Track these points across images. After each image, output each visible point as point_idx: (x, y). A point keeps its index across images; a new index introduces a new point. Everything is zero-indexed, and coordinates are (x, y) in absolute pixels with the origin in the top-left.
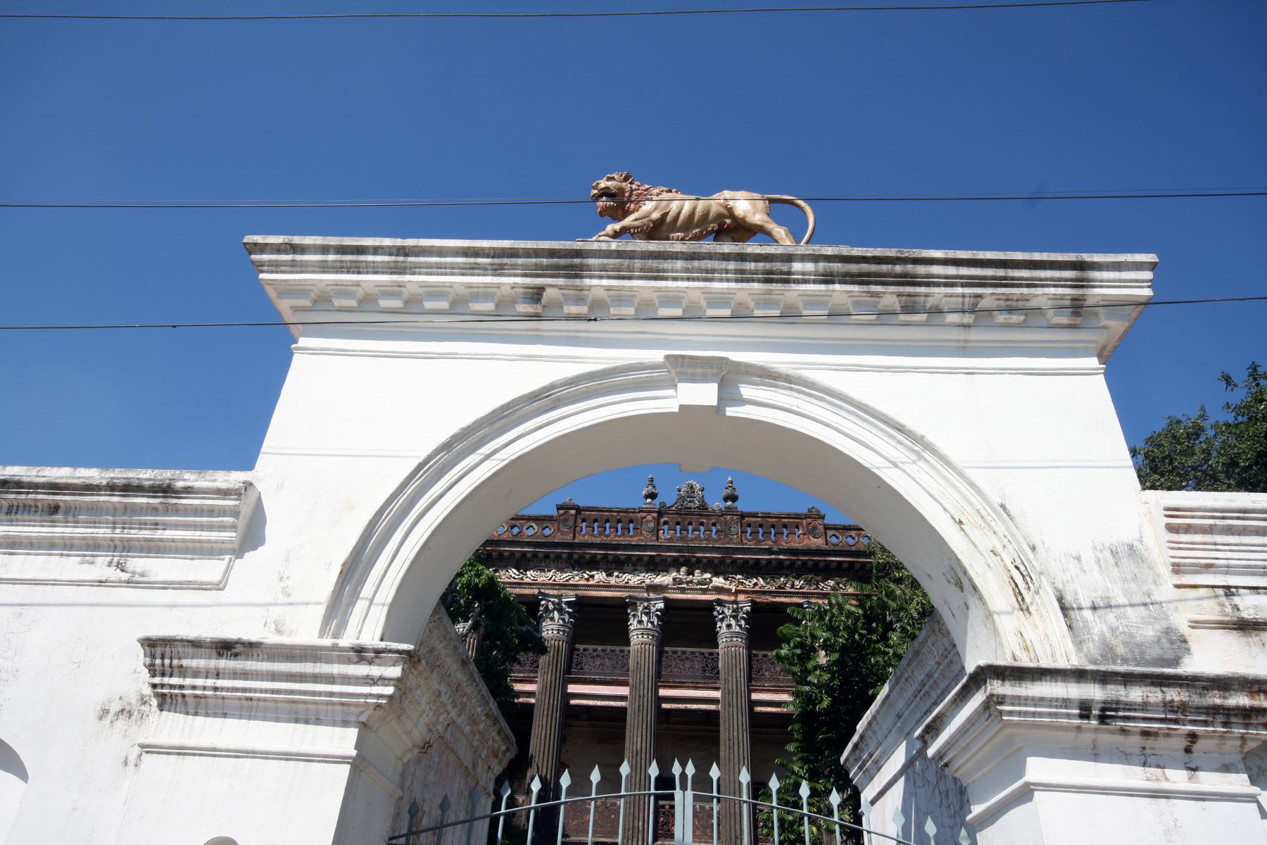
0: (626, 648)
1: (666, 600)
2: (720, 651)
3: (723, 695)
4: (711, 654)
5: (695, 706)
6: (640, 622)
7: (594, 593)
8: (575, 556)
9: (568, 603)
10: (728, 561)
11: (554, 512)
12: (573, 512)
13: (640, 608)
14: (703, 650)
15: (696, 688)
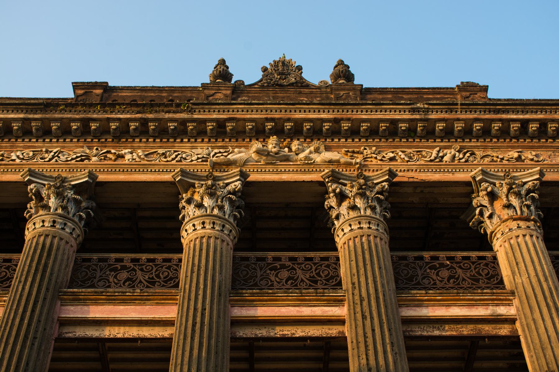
0: (176, 256)
1: (247, 184)
2: (342, 253)
3: (353, 311)
4: (326, 259)
5: (300, 332)
6: (200, 206)
7: (122, 177)
8: (93, 126)
9: (78, 189)
10: (345, 126)
11: (69, 94)
12: (99, 91)
13: (202, 190)
14: (311, 254)
15: (302, 302)
